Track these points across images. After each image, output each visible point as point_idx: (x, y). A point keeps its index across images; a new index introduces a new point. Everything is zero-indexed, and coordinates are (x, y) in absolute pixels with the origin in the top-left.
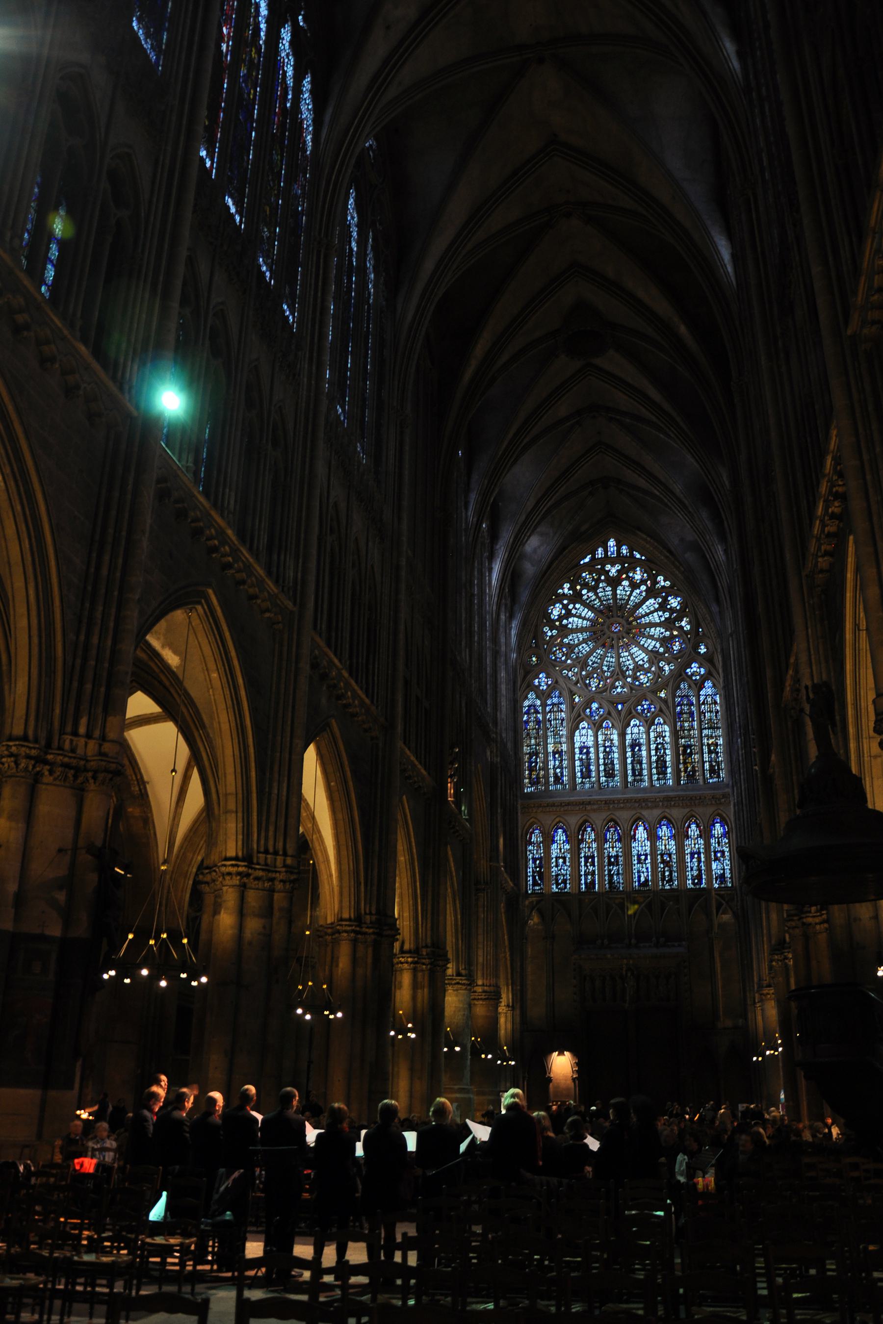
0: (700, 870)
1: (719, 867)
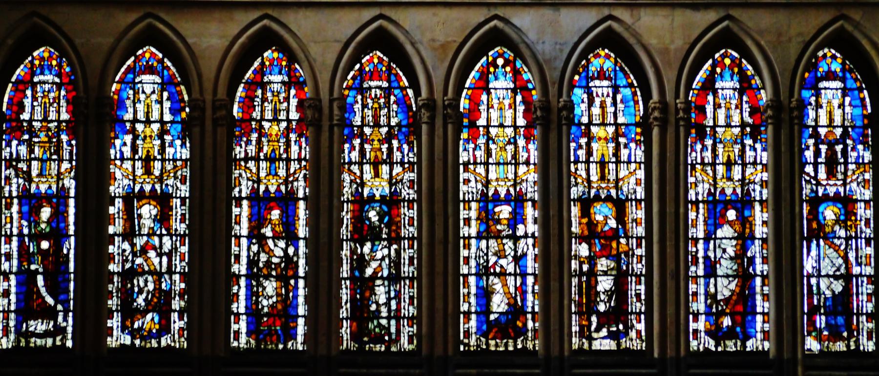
0: (744, 276)
1: (827, 268)
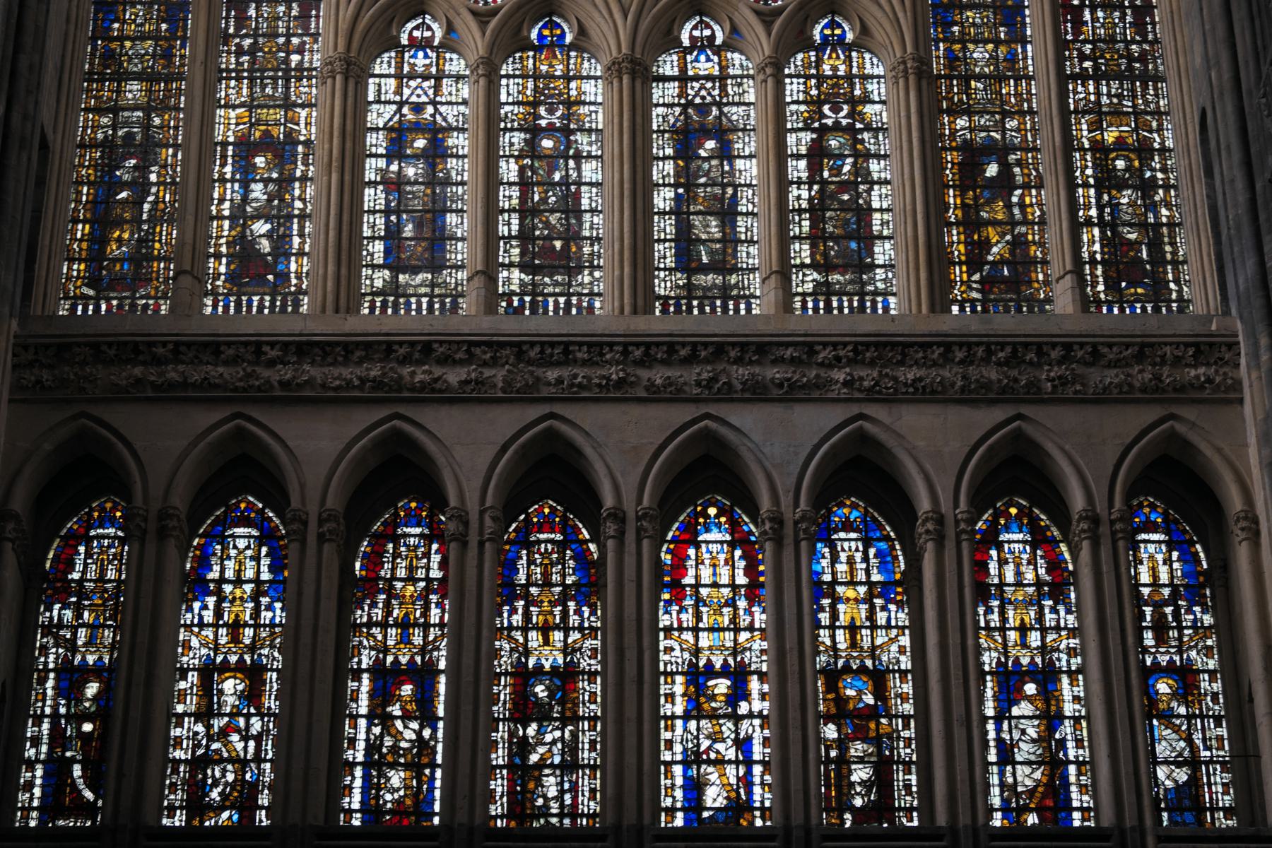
0: (1053, 762)
